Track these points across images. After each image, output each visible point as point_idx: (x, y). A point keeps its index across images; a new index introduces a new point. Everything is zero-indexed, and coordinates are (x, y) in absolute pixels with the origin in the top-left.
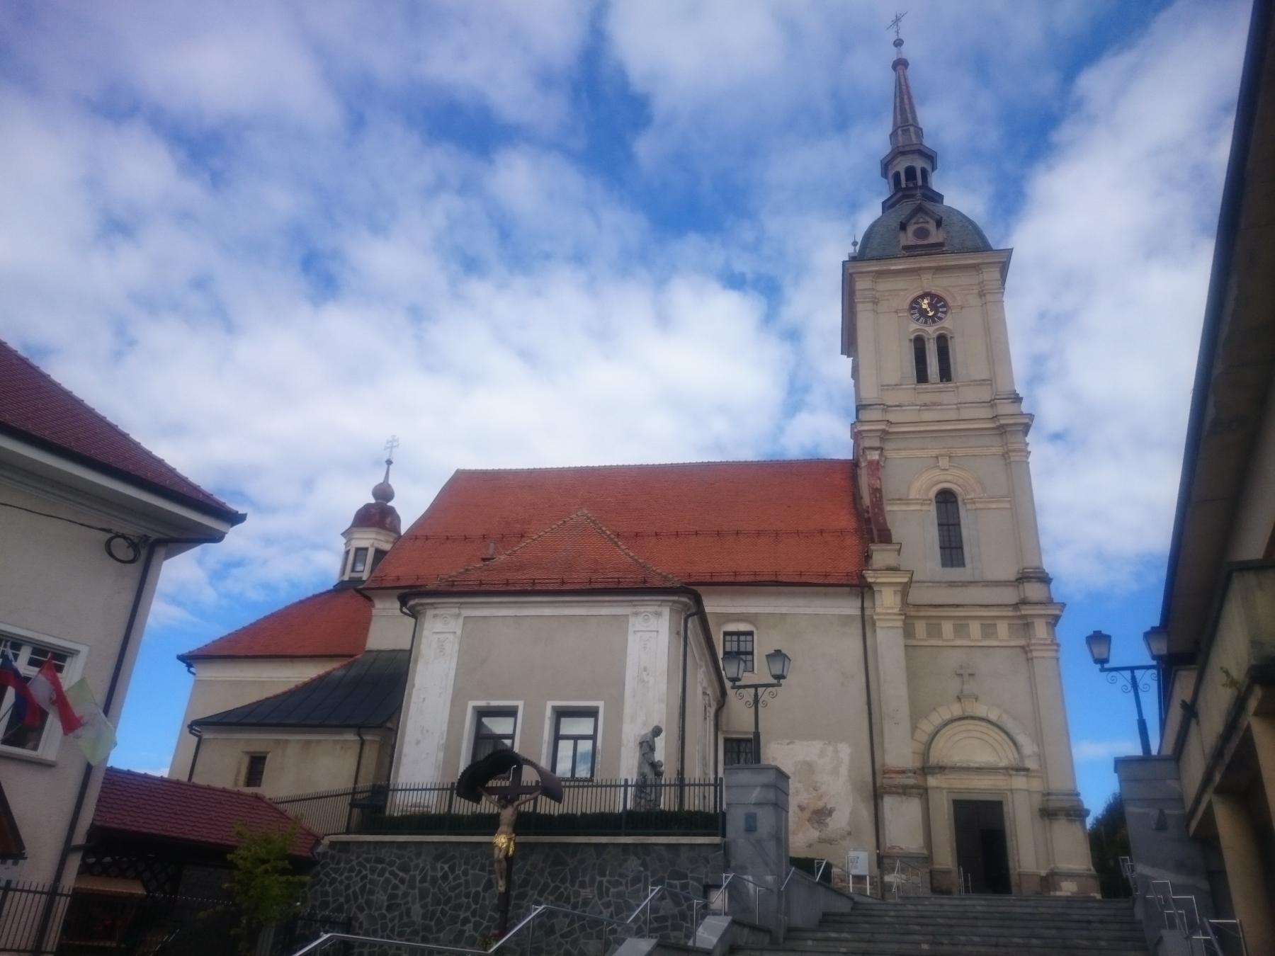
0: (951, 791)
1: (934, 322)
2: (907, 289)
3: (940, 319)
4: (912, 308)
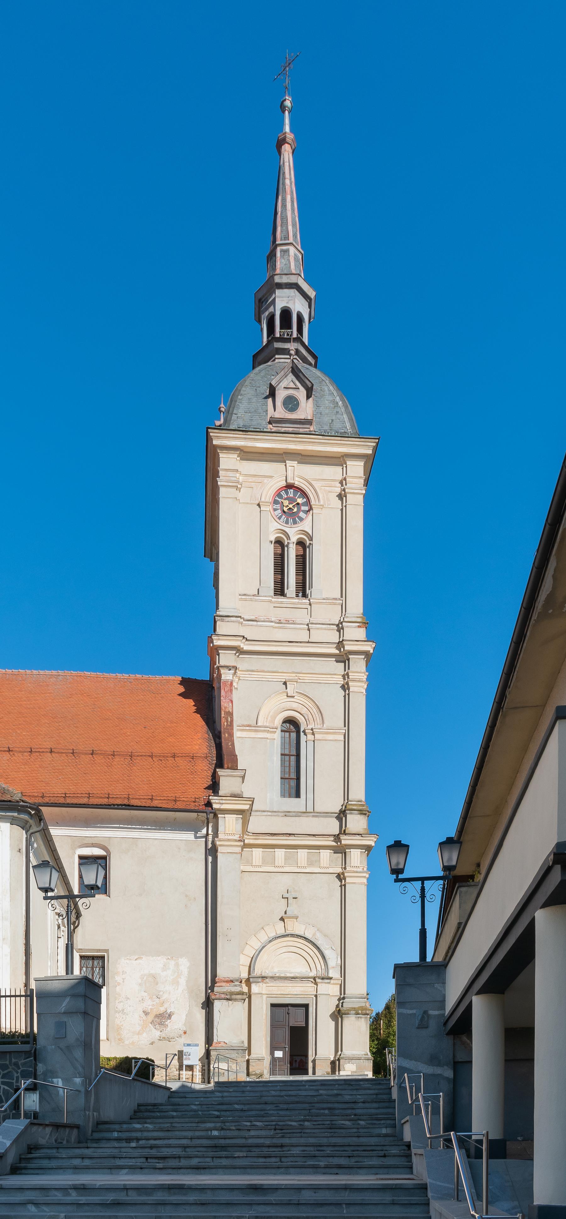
0: (269, 996)
1: (295, 522)
2: (274, 476)
3: (301, 519)
4: (275, 502)
